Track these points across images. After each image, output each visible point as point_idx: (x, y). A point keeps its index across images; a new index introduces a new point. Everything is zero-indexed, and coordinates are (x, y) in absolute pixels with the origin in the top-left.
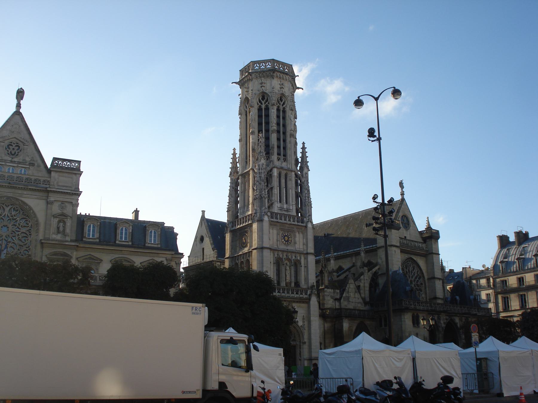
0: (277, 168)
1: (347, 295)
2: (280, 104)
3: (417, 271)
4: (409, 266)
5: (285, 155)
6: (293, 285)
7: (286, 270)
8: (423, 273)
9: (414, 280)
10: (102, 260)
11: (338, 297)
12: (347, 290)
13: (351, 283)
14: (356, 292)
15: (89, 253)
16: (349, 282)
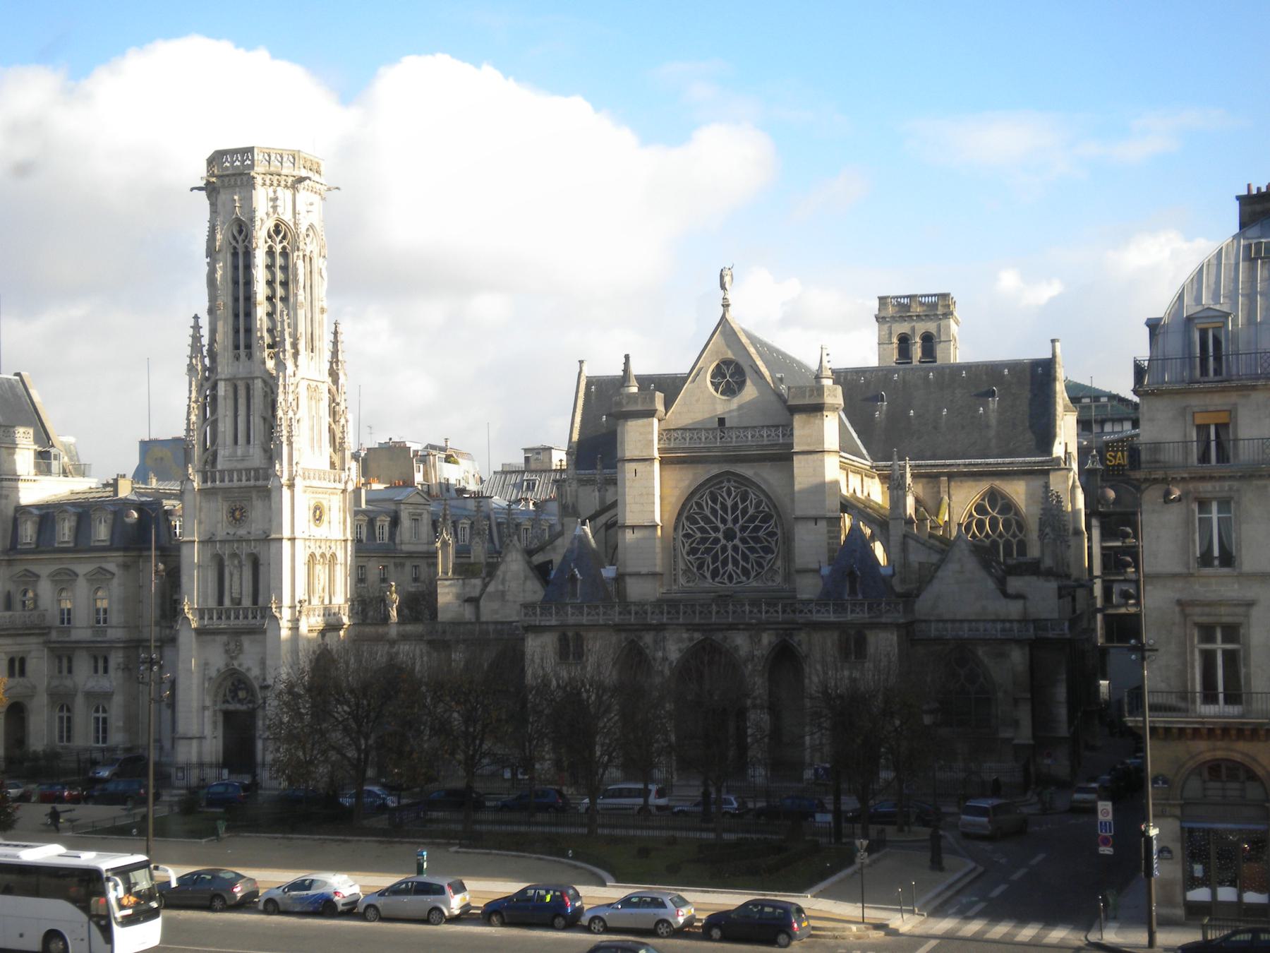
0: (225, 380)
1: (501, 587)
2: (237, 242)
3: (754, 502)
4: (724, 495)
5: (248, 346)
6: (247, 602)
7: (231, 575)
8: (775, 507)
9: (743, 529)
10: (38, 576)
11: (476, 593)
12: (501, 577)
13: (512, 561)
14: (526, 578)
15: (23, 568)
16: (509, 559)
